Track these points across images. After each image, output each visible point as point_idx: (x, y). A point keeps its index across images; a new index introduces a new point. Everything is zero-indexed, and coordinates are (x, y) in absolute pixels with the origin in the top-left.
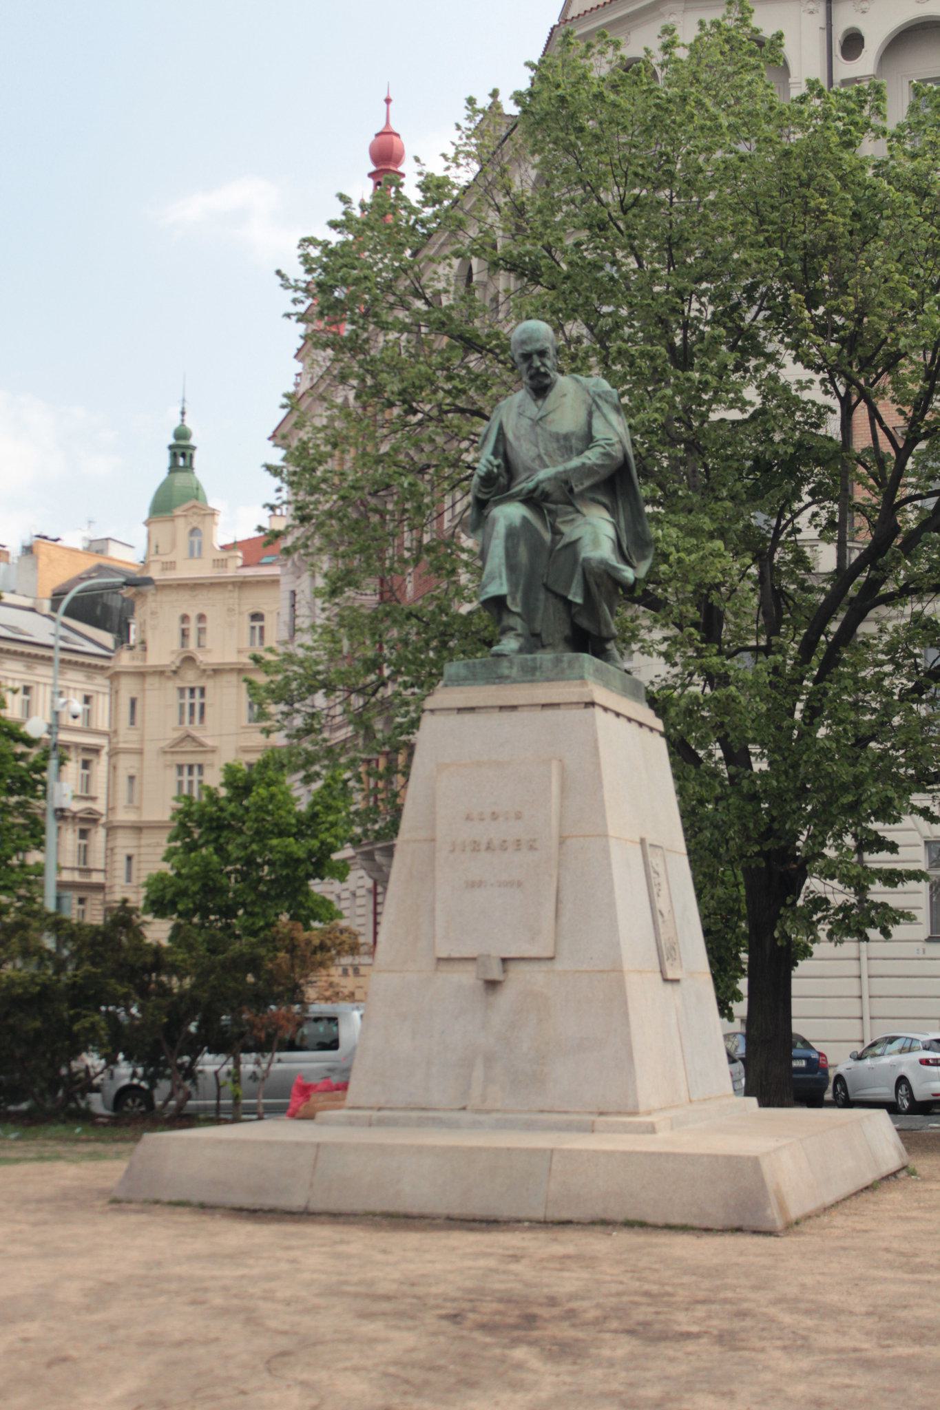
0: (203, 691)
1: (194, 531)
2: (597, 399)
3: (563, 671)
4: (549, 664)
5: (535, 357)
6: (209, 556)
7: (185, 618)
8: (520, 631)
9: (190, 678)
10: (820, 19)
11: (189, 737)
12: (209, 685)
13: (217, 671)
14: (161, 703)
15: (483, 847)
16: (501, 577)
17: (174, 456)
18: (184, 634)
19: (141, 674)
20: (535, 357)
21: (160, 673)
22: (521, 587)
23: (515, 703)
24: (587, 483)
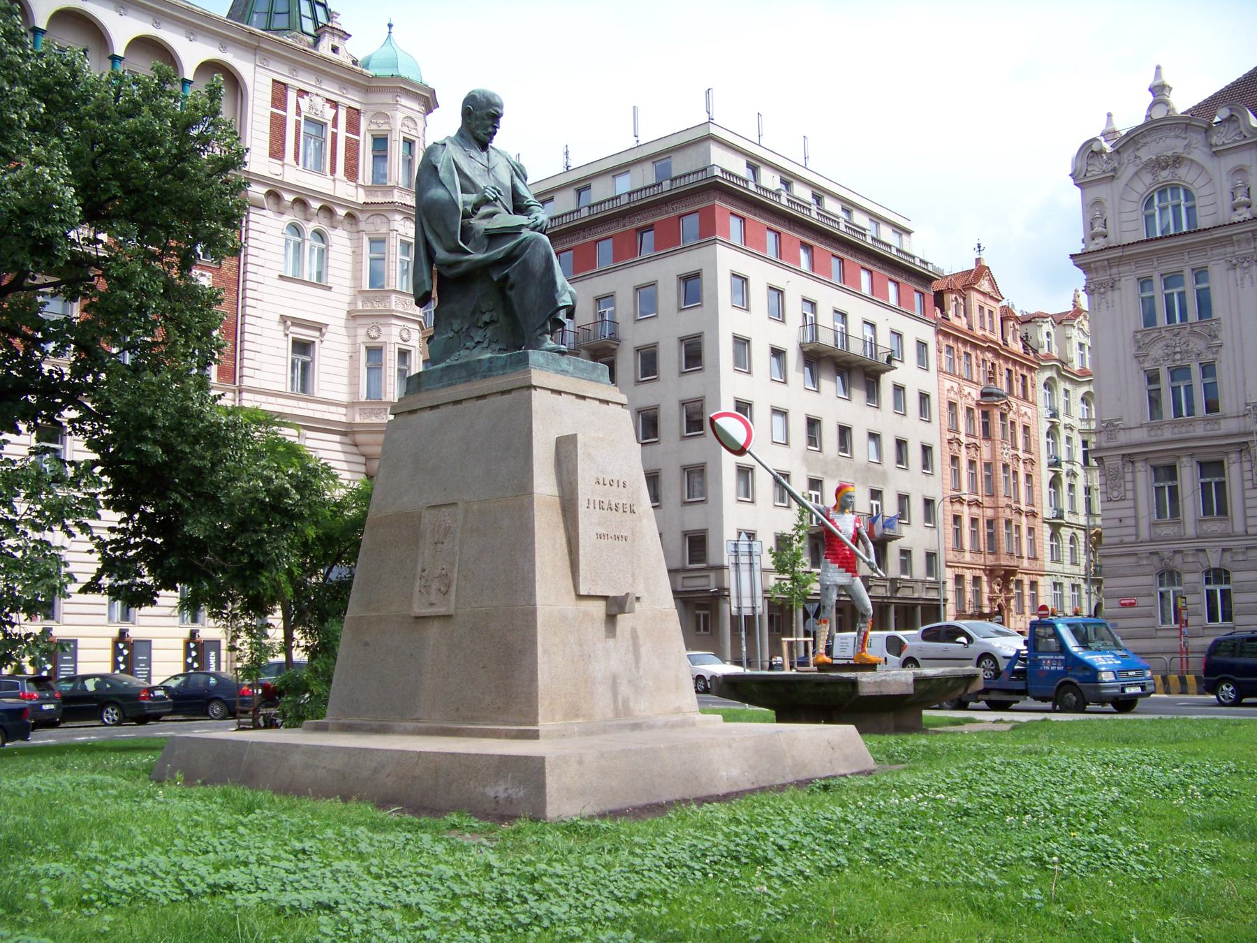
15: (605, 507)
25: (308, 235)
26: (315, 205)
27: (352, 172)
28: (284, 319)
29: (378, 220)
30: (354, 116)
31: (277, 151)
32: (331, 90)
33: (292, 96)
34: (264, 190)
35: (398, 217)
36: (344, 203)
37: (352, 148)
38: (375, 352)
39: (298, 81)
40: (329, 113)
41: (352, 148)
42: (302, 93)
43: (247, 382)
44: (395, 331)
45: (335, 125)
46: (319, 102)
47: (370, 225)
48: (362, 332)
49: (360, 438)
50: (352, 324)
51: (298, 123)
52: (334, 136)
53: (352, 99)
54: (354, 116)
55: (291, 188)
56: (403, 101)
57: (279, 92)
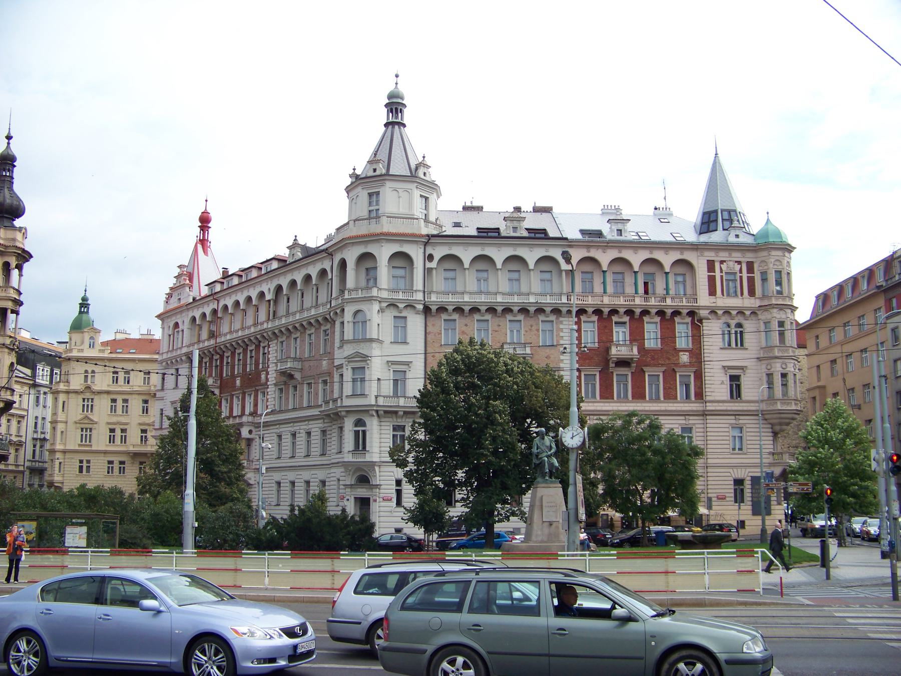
0: (92, 399)
1: (92, 338)
6: (98, 346)
7: (86, 371)
9: (88, 395)
10: (422, 250)
11: (87, 417)
12: (96, 398)
13: (100, 393)
14: (75, 406)
17: (81, 308)
18: (86, 377)
19: (68, 392)
21: (76, 392)
25: (733, 326)
26: (734, 313)
27: (752, 293)
28: (724, 367)
29: (766, 313)
30: (750, 267)
31: (712, 292)
32: (737, 256)
33: (717, 265)
34: (708, 311)
35: (775, 310)
36: (748, 309)
37: (751, 281)
38: (770, 376)
39: (723, 255)
40: (737, 267)
41: (751, 281)
42: (722, 262)
43: (708, 398)
44: (778, 365)
45: (741, 271)
46: (731, 264)
47: (764, 316)
48: (764, 366)
49: (767, 417)
50: (759, 363)
51: (722, 277)
52: (741, 278)
53: (749, 257)
54: (750, 267)
55: (720, 308)
56: (774, 253)
57: (711, 265)
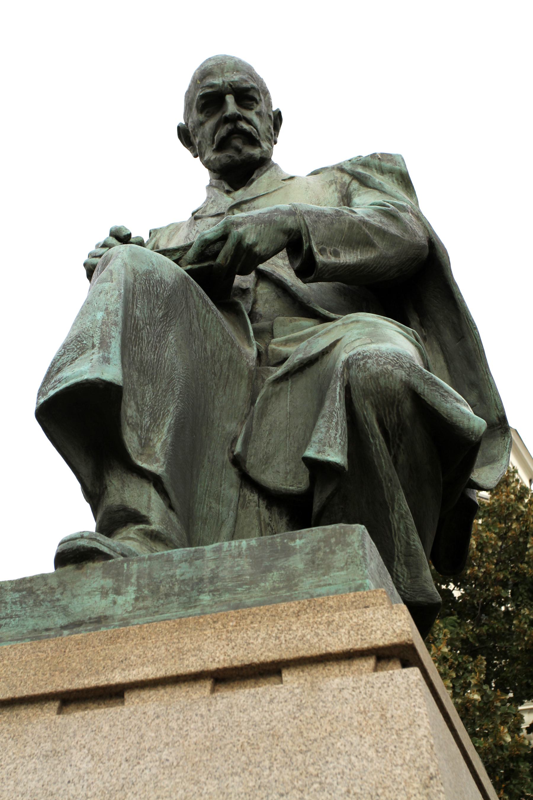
2: (360, 170)
3: (290, 581)
4: (245, 564)
5: (230, 99)
8: (155, 526)
16: (104, 345)
20: (230, 99)
22: (169, 420)
23: (118, 678)
24: (348, 258)
